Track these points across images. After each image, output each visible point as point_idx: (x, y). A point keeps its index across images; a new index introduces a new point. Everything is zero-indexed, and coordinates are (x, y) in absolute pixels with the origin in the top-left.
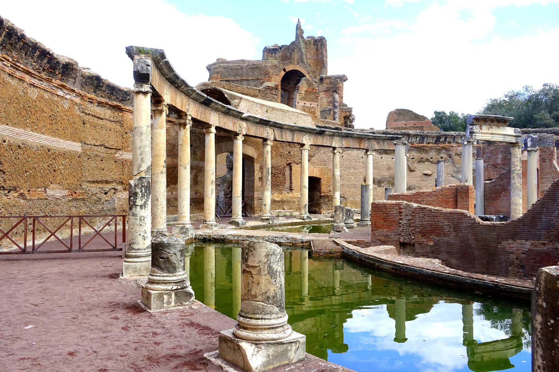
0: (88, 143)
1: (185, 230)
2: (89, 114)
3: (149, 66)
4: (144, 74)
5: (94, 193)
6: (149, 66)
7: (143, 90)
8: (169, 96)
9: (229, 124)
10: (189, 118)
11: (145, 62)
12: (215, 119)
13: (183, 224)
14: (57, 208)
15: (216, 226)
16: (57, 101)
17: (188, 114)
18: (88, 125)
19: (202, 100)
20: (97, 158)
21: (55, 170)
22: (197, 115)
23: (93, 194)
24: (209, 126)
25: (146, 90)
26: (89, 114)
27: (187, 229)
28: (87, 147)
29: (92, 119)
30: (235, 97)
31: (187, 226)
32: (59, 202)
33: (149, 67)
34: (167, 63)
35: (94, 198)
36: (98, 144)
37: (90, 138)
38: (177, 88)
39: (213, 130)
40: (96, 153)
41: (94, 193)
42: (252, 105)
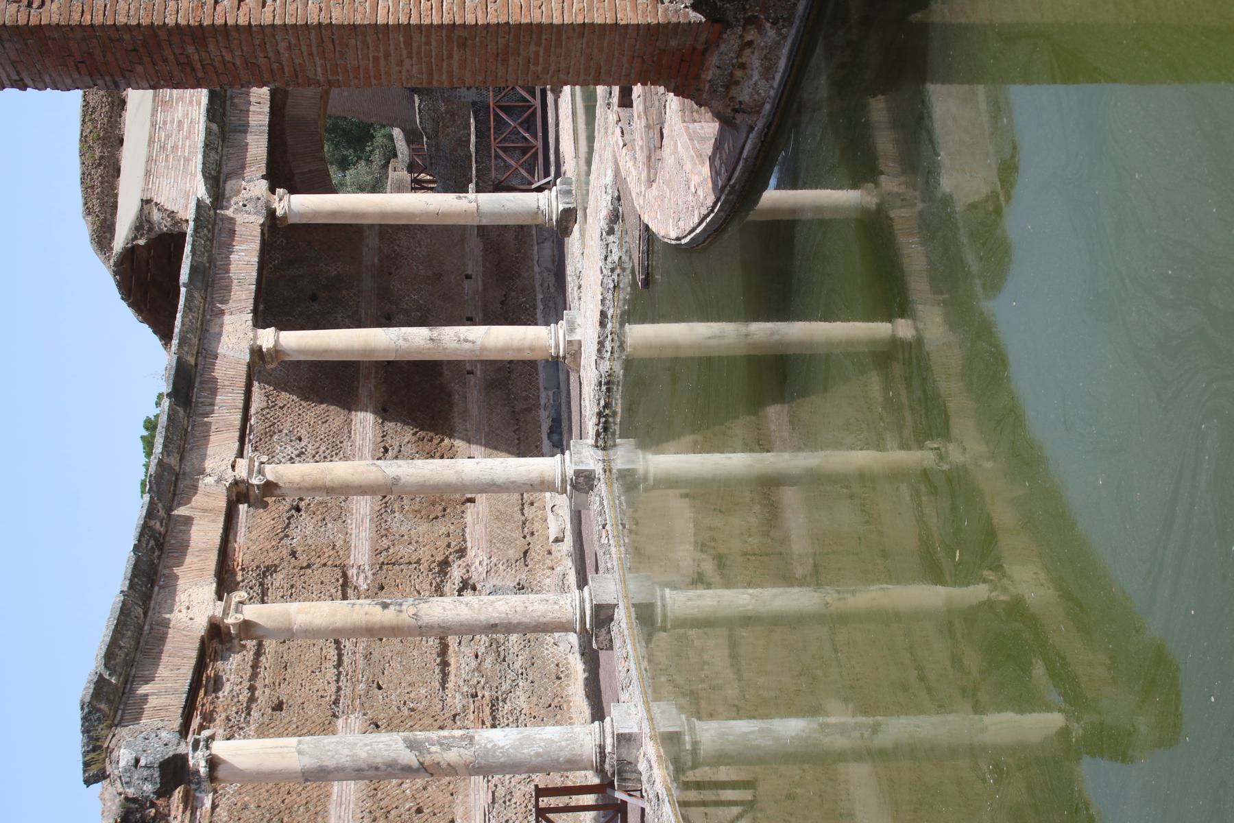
0: (333, 688)
1: (581, 480)
2: (252, 689)
3: (137, 761)
4: (162, 776)
5: (474, 664)
6: (137, 761)
7: (203, 770)
8: (194, 604)
9: (244, 260)
10: (242, 464)
11: (126, 770)
12: (238, 336)
13: (564, 481)
14: (518, 795)
15: (572, 330)
16: (230, 812)
17: (229, 476)
18: (283, 692)
19: (181, 412)
20: (376, 656)
21: (419, 811)
22: (228, 427)
23: (478, 669)
24: (257, 353)
25: (203, 763)
26: (252, 689)
27: (578, 473)
28: (346, 691)
29: (266, 676)
30: (142, 223)
31: (570, 473)
32: (501, 792)
33: (143, 762)
34: (109, 656)
35: (487, 664)
36: (332, 653)
37: (320, 684)
38: (160, 546)
39: (267, 338)
40: (361, 663)
41: (474, 664)
42: (163, 148)
